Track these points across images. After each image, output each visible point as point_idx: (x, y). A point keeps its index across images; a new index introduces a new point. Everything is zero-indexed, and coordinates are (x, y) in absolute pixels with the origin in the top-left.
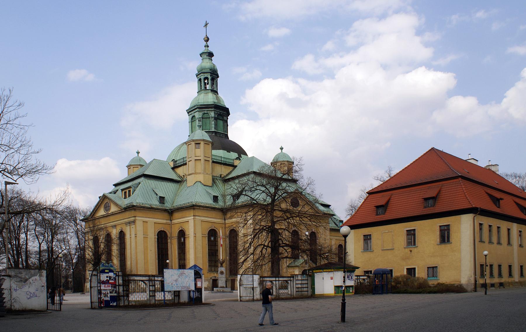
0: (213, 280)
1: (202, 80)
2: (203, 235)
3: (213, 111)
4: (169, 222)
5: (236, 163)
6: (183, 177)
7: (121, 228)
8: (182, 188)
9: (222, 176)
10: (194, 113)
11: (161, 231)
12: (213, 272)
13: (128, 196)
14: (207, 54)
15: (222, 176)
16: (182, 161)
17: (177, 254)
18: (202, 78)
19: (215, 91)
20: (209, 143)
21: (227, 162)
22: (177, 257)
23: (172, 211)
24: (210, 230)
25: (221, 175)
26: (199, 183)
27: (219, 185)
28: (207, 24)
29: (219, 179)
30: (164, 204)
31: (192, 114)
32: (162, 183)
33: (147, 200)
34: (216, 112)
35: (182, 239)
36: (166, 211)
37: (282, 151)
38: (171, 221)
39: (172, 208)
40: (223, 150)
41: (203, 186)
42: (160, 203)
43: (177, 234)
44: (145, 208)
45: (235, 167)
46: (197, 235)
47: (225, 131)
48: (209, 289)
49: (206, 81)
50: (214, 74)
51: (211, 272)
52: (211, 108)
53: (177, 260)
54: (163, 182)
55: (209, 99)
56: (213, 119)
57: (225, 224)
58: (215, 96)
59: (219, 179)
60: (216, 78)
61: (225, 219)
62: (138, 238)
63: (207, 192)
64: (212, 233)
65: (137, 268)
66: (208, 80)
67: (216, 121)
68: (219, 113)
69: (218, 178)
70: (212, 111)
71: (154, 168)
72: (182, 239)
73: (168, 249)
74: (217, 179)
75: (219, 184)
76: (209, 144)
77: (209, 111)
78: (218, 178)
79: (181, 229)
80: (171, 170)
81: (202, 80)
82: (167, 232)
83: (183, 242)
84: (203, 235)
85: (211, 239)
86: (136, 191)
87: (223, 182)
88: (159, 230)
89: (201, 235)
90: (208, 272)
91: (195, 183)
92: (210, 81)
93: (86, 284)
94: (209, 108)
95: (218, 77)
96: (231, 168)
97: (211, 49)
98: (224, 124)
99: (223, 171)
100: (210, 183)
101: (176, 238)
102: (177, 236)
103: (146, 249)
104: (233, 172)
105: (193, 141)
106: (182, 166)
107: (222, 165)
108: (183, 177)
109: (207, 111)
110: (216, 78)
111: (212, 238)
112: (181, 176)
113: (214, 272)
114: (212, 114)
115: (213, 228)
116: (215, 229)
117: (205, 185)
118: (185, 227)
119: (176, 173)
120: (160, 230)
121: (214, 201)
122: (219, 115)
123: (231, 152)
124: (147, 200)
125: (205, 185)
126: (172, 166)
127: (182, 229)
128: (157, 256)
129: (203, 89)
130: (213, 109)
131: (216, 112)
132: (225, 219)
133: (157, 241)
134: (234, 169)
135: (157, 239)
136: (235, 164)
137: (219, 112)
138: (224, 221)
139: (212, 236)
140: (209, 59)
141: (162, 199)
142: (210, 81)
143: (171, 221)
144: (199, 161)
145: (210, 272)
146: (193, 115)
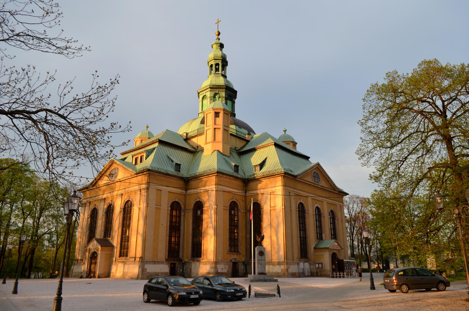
0: (233, 262)
1: (214, 66)
2: (225, 208)
4: (184, 191)
9: (237, 149)
11: (175, 201)
14: (219, 45)
17: (191, 230)
19: (224, 76)
21: (241, 136)
22: (191, 233)
23: (188, 180)
25: (236, 148)
32: (177, 151)
33: (163, 166)
34: (227, 93)
35: (199, 212)
36: (182, 178)
37: (285, 133)
38: (186, 190)
39: (188, 176)
40: (235, 125)
41: (222, 155)
42: (176, 170)
43: (192, 206)
45: (248, 141)
48: (229, 275)
49: (217, 67)
50: (225, 62)
51: (231, 253)
52: (223, 88)
53: (191, 237)
55: (221, 81)
57: (245, 197)
58: (225, 79)
61: (246, 190)
64: (233, 206)
66: (219, 66)
69: (233, 150)
72: (199, 212)
76: (228, 114)
78: (233, 150)
79: (198, 200)
80: (184, 141)
81: (214, 66)
82: (181, 203)
84: (225, 208)
87: (238, 155)
88: (172, 202)
89: (223, 208)
90: (228, 252)
93: (73, 266)
94: (221, 88)
95: (227, 65)
96: (244, 143)
97: (221, 41)
99: (239, 144)
100: (228, 153)
101: (191, 210)
102: (192, 208)
104: (247, 146)
106: (196, 137)
109: (219, 91)
113: (234, 253)
114: (223, 94)
116: (236, 201)
117: (223, 155)
118: (204, 198)
119: (189, 144)
124: (163, 166)
125: (223, 155)
127: (200, 200)
128: (168, 232)
131: (227, 93)
132: (246, 190)
141: (178, 166)
143: (186, 190)
145: (230, 253)
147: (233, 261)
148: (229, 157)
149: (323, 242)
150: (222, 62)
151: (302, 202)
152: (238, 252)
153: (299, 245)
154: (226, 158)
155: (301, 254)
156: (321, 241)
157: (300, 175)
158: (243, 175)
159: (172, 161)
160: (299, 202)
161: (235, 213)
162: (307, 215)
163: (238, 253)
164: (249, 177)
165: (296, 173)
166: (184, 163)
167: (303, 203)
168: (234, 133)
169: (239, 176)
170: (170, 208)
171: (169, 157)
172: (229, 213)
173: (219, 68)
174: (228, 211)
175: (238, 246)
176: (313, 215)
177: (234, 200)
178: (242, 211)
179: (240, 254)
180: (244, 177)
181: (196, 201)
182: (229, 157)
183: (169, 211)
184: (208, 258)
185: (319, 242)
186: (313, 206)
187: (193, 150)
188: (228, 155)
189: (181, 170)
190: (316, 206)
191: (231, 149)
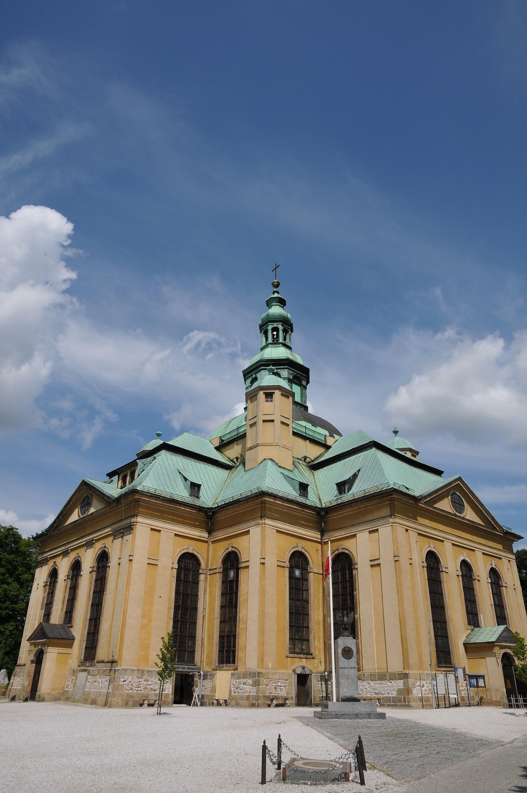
0: (298, 674)
3: (287, 370)
5: (330, 441)
6: (235, 460)
7: (104, 545)
8: (233, 476)
9: (308, 460)
10: (255, 373)
11: (187, 553)
12: (299, 656)
13: (129, 482)
15: (308, 460)
16: (236, 432)
18: (270, 328)
20: (288, 395)
24: (293, 552)
26: (270, 462)
27: (304, 473)
28: (278, 267)
29: (302, 464)
30: (198, 498)
31: (252, 375)
36: (200, 509)
41: (277, 467)
44: (159, 498)
46: (266, 561)
47: (304, 401)
49: (275, 333)
51: (295, 655)
54: (199, 463)
56: (287, 380)
59: (302, 464)
60: (289, 330)
62: (134, 565)
63: (287, 477)
65: (122, 637)
67: (290, 384)
68: (295, 373)
70: (285, 370)
71: (185, 441)
72: (232, 574)
73: (197, 596)
74: (299, 463)
75: (303, 470)
77: (279, 370)
78: (300, 462)
79: (230, 549)
83: (232, 580)
85: (295, 573)
86: (144, 471)
87: (310, 470)
88: (183, 552)
90: (288, 653)
91: (261, 463)
92: (281, 333)
96: (321, 450)
98: (302, 391)
103: (150, 590)
105: (261, 388)
107: (308, 441)
108: (235, 460)
110: (289, 330)
111: (297, 573)
112: (232, 459)
113: (302, 656)
115: (300, 550)
116: (303, 551)
120: (185, 551)
121: (301, 494)
122: (294, 377)
123: (318, 427)
126: (217, 444)
127: (234, 549)
128: (172, 611)
129: (270, 340)
130: (287, 367)
131: (292, 372)
133: (176, 576)
134: (327, 451)
135: (176, 570)
136: (329, 443)
137: (295, 372)
138: (320, 537)
139: (298, 567)
140: (280, 306)
142: (281, 333)
144: (271, 424)
145: (292, 655)
146: (254, 376)
147: (299, 671)
148: (291, 471)
149: (482, 631)
150: (282, 325)
151: (433, 549)
152: (309, 653)
153: (433, 637)
154: (286, 472)
155: (438, 657)
156: (477, 629)
157: (426, 497)
158: (318, 502)
159: (186, 479)
160: (428, 549)
161: (302, 574)
162: (444, 576)
163: (309, 656)
164: (329, 505)
165: (417, 493)
166: (210, 485)
167: (436, 551)
168: (303, 432)
169: (308, 503)
170: (176, 566)
171: (180, 473)
172: (290, 574)
173: (278, 335)
174: (287, 570)
175: (308, 640)
176: (458, 576)
177: (300, 549)
178: (315, 570)
179: (313, 658)
180: (319, 506)
181: (227, 551)
182: (291, 471)
183: (175, 571)
184: (247, 666)
185: (472, 630)
186: (456, 558)
187: (228, 463)
188: (291, 467)
189: (201, 494)
190: (462, 558)
191: (296, 460)
